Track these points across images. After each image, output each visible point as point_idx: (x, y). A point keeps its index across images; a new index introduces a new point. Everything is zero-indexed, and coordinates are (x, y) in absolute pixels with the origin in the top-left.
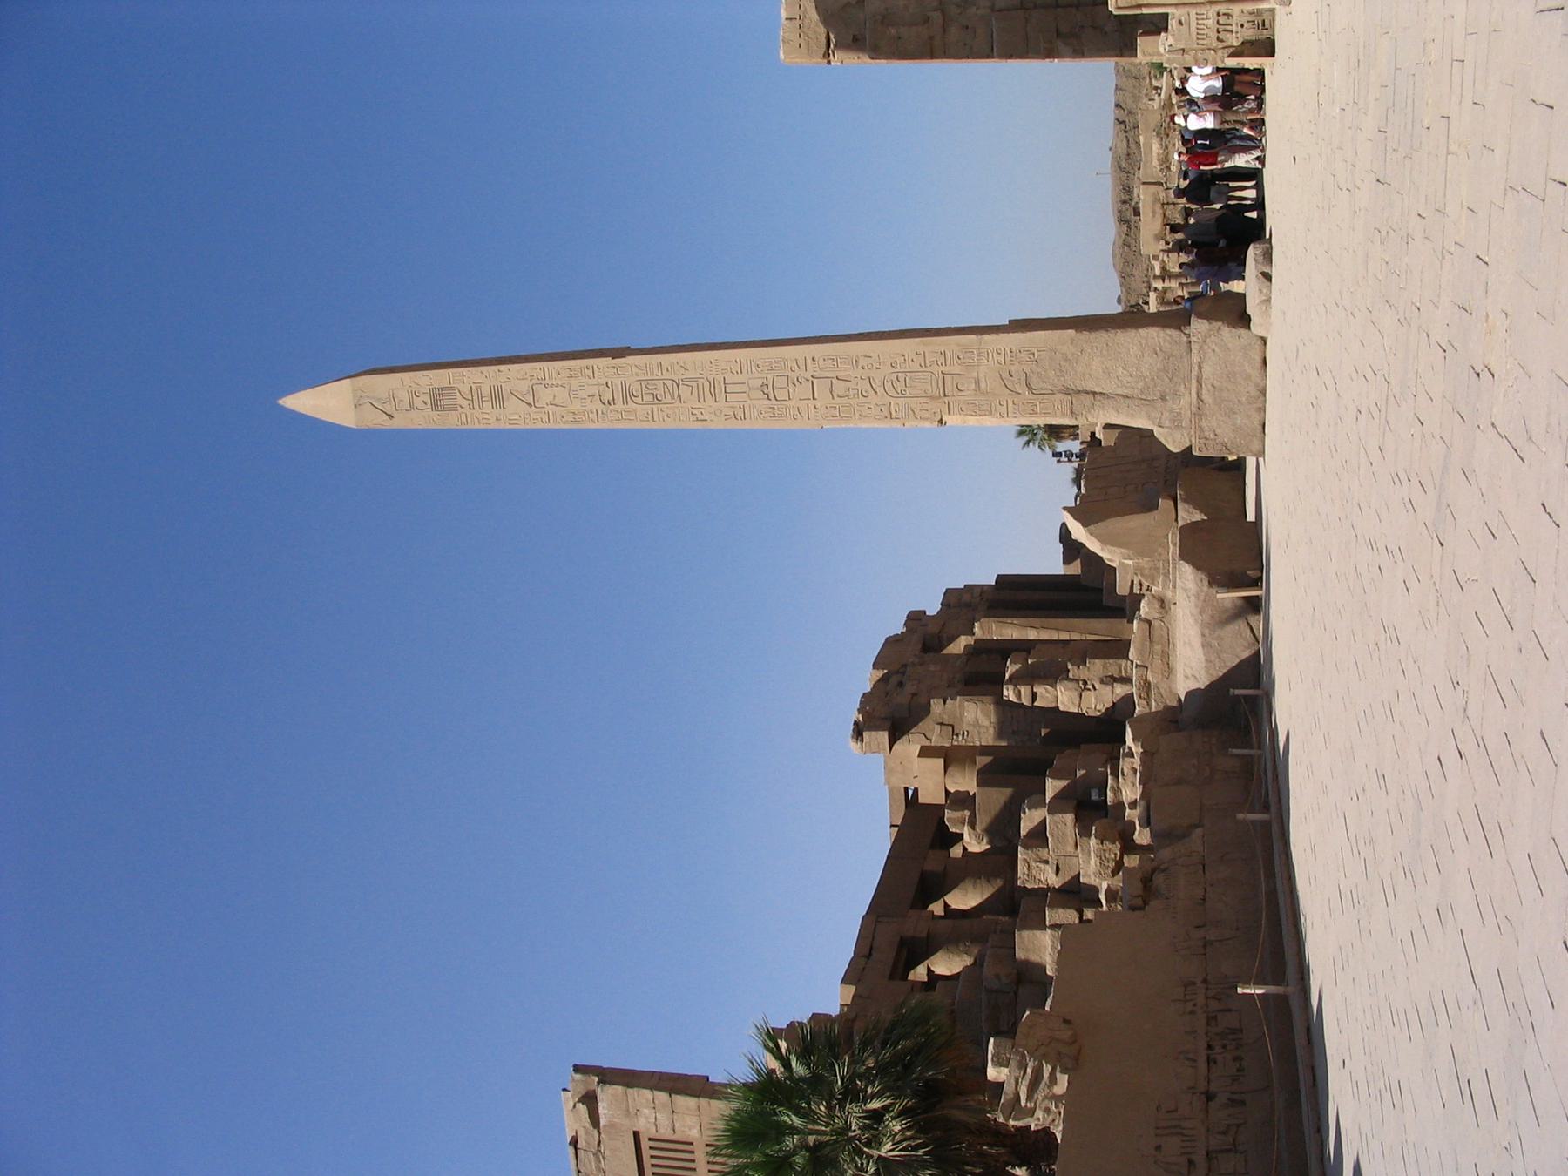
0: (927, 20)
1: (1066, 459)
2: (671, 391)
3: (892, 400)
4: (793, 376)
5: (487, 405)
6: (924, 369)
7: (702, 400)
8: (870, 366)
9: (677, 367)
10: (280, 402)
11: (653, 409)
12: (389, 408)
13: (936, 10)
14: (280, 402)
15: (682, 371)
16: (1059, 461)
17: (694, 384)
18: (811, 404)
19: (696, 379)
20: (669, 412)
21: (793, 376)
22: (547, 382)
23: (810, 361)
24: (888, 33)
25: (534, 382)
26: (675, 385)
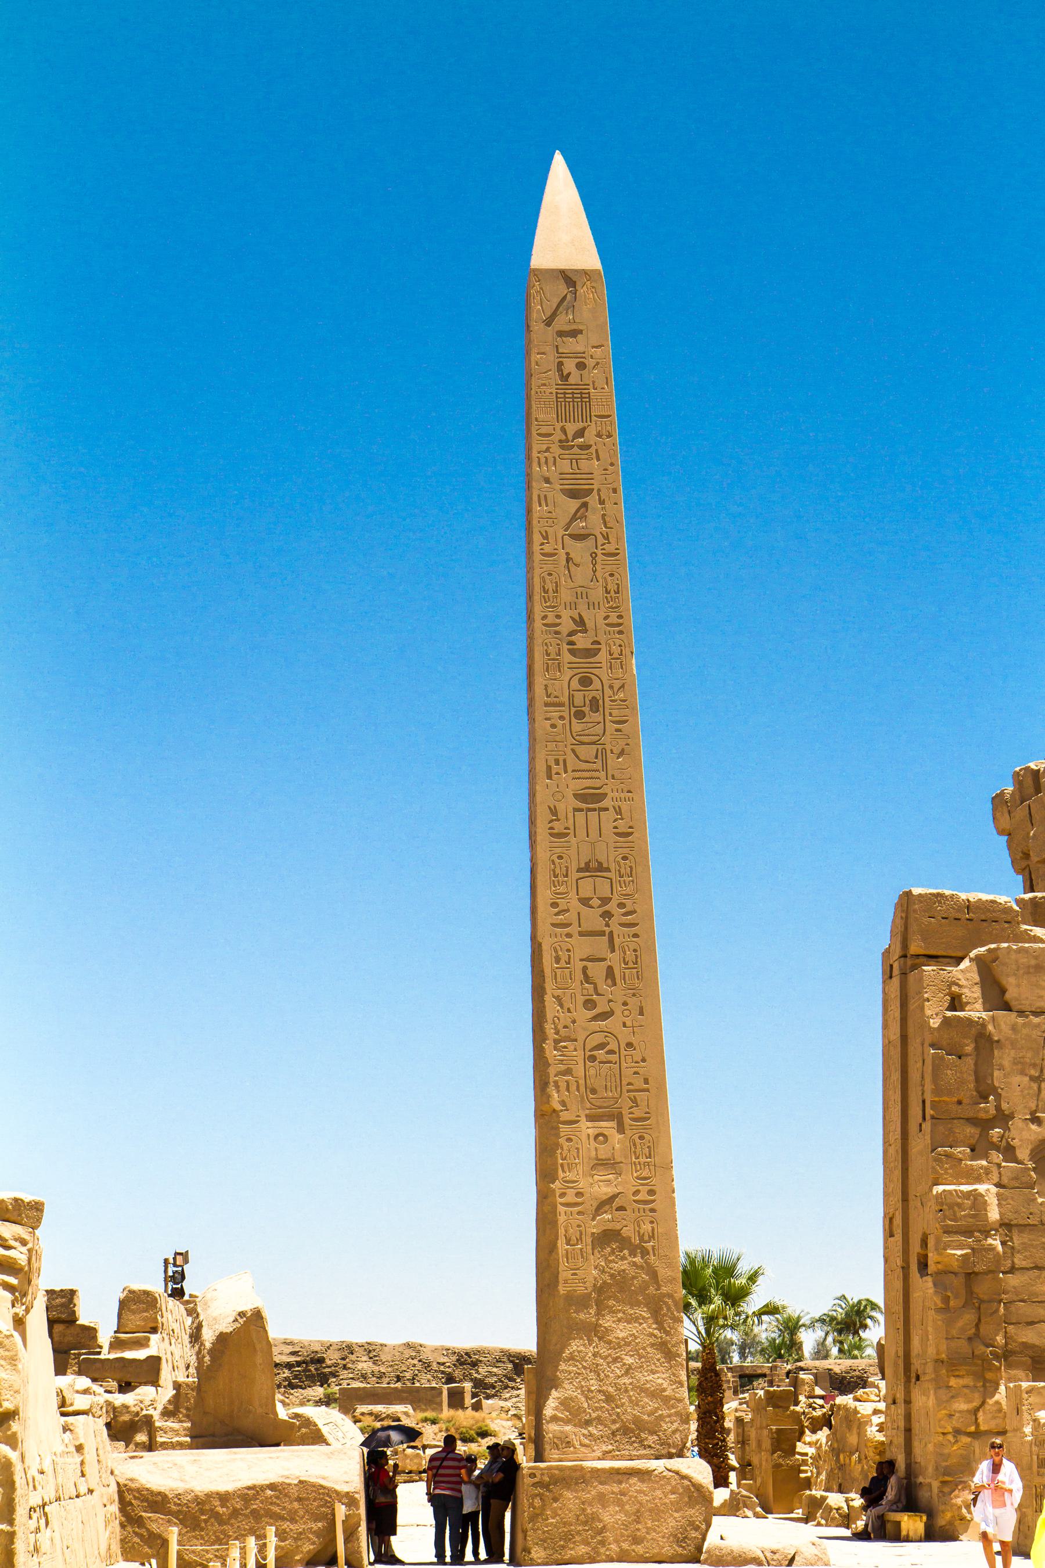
0: (985, 1098)
1: (170, 1273)
2: (582, 733)
3: (580, 1042)
4: (612, 907)
5: (565, 466)
6: (625, 1088)
7: (577, 774)
8: (626, 1013)
9: (622, 743)
10: (558, 159)
11: (562, 705)
12: (562, 322)
13: (998, 1108)
14: (557, 151)
15: (617, 751)
16: (166, 1261)
17: (598, 765)
18: (574, 929)
19: (605, 767)
20: (560, 727)
21: (612, 907)
22: (600, 558)
23: (634, 930)
24: (966, 1041)
25: (600, 537)
26: (598, 738)
